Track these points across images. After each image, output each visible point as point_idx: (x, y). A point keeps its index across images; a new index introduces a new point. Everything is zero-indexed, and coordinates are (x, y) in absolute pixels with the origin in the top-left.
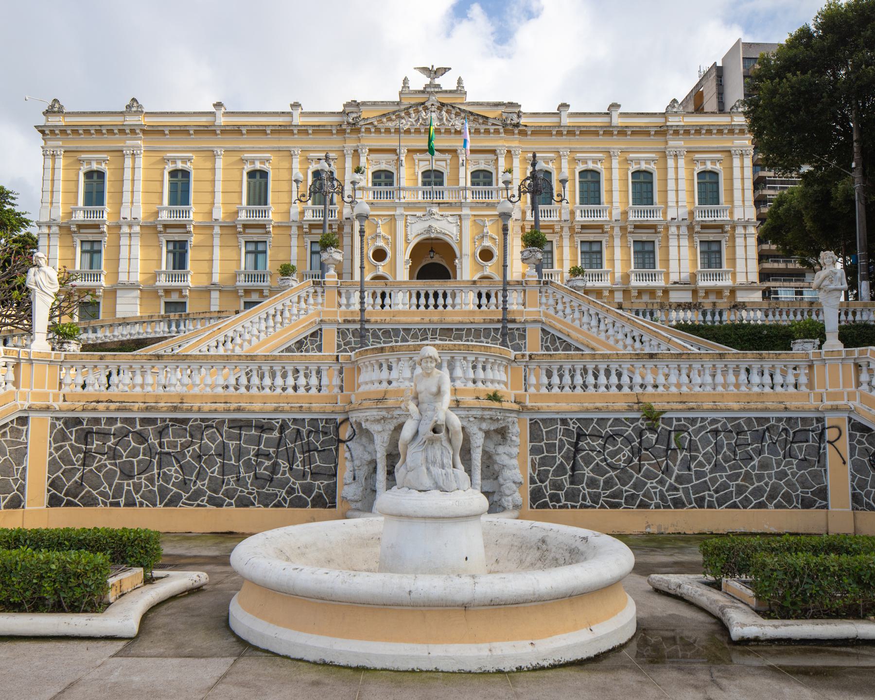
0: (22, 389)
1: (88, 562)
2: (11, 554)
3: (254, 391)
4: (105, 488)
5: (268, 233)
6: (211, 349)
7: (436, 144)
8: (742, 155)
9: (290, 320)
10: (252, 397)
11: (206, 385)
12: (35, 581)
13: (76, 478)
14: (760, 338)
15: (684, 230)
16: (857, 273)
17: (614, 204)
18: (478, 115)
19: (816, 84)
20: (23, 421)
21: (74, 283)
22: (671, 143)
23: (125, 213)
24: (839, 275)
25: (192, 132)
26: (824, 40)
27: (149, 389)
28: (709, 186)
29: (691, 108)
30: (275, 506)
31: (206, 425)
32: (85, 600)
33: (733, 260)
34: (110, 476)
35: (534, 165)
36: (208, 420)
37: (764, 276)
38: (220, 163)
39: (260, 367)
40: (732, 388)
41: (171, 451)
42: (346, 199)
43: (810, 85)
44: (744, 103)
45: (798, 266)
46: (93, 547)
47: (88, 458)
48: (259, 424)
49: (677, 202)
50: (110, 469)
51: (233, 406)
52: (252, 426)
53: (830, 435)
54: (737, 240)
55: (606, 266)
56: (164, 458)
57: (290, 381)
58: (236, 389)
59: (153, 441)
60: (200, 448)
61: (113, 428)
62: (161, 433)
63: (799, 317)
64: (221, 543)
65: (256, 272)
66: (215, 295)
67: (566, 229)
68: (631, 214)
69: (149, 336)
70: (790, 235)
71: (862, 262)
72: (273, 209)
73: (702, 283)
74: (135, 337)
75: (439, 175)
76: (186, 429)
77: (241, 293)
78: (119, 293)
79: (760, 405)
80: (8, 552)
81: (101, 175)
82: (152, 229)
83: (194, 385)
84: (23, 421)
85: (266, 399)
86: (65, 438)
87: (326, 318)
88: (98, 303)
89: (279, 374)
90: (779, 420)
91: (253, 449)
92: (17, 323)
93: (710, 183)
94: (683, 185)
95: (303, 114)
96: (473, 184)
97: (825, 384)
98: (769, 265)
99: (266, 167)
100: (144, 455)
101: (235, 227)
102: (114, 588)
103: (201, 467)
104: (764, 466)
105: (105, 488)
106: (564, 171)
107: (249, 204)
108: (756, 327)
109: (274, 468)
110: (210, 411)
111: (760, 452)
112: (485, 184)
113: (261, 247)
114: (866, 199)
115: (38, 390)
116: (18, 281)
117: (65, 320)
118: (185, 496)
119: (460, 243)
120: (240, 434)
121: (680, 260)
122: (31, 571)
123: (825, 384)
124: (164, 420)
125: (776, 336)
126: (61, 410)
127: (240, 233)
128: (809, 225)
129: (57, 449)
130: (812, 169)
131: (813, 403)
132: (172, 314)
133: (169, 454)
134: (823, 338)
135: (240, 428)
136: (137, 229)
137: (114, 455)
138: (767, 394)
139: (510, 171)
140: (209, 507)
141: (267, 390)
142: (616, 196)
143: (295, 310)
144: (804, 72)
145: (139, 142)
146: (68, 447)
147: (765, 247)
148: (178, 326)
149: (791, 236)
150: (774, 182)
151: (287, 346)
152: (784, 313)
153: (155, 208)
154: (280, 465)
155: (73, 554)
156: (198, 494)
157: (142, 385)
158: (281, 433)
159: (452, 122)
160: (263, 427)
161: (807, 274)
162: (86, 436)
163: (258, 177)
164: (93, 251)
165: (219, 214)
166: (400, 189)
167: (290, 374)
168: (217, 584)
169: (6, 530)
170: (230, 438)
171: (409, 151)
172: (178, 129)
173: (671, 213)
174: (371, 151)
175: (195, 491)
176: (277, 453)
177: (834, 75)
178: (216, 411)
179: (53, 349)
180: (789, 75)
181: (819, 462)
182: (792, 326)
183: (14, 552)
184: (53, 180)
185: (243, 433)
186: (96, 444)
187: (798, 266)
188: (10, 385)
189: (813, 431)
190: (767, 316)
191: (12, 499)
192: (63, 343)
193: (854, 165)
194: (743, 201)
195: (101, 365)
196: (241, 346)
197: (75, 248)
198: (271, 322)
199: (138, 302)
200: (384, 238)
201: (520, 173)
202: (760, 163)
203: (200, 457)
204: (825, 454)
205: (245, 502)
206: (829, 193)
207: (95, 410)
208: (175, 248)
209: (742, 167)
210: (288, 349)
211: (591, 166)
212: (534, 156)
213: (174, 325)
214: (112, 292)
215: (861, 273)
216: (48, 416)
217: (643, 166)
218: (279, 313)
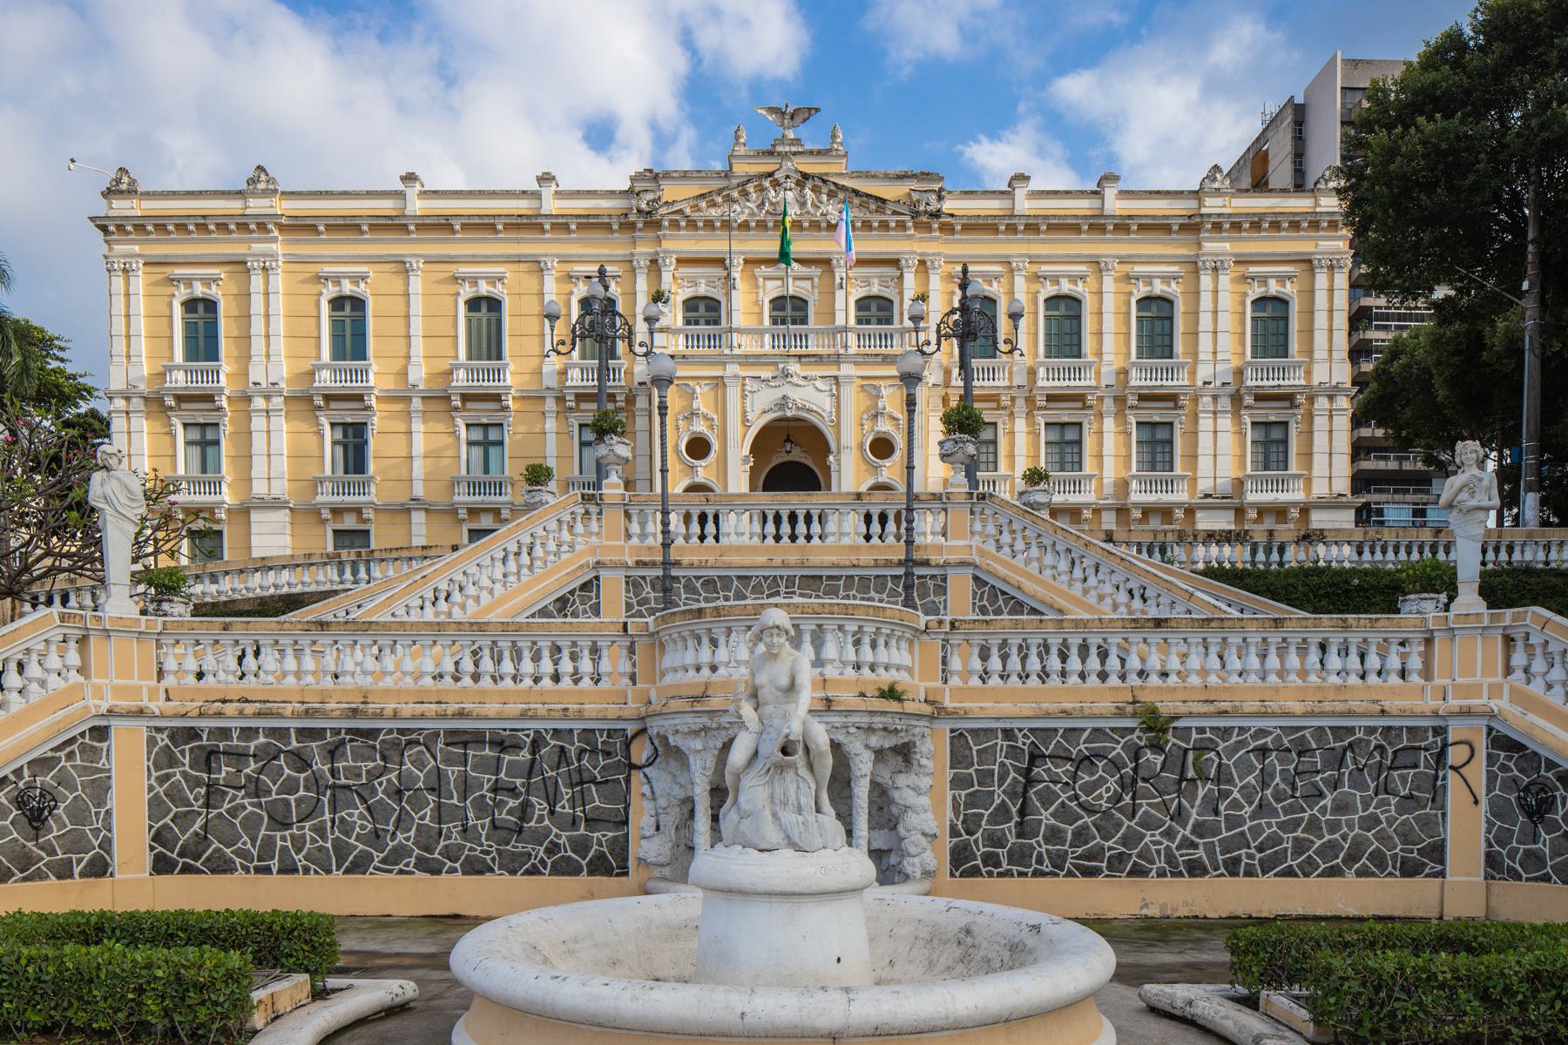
0: (94, 680)
1: (216, 966)
2: (88, 953)
3: (486, 682)
4: (245, 843)
5: (505, 409)
6: (412, 612)
7: (799, 247)
8: (1331, 268)
9: (545, 563)
10: (484, 692)
11: (405, 673)
12: (131, 996)
13: (196, 827)
14: (1347, 591)
15: (1225, 403)
16: (1518, 478)
17: (1105, 357)
18: (868, 196)
19: (1466, 136)
20: (101, 733)
21: (172, 498)
22: (1208, 246)
23: (257, 374)
24: (1486, 483)
25: (365, 228)
26: (1486, 54)
27: (309, 679)
28: (1272, 325)
29: (1246, 181)
30: (527, 873)
31: (406, 740)
32: (215, 1026)
33: (1307, 456)
34: (251, 824)
35: (963, 286)
36: (412, 731)
37: (1361, 482)
38: (417, 284)
39: (494, 642)
40: (1293, 677)
41: (351, 782)
42: (638, 349)
43: (1458, 138)
44: (1338, 173)
45: (1420, 466)
46: (225, 940)
47: (213, 794)
48: (498, 739)
49: (1215, 353)
50: (252, 813)
51: (452, 708)
52: (484, 742)
53: (1455, 755)
54: (1317, 420)
55: (1089, 467)
56: (340, 795)
57: (547, 666)
58: (457, 679)
59: (321, 766)
60: (399, 777)
61: (252, 745)
62: (333, 753)
63: (1415, 556)
64: (440, 932)
65: (486, 478)
66: (418, 518)
67: (1020, 403)
68: (1134, 373)
69: (307, 589)
70: (1408, 412)
71: (1529, 460)
72: (512, 367)
73: (1255, 496)
74: (285, 590)
75: (800, 304)
76: (374, 747)
77: (463, 514)
78: (255, 516)
79: (1339, 707)
80: (84, 950)
81: (211, 305)
82: (305, 402)
83: (384, 673)
84: (101, 733)
85: (506, 696)
86: (173, 762)
87: (602, 559)
88: (220, 533)
89: (527, 655)
90: (1371, 730)
91: (487, 779)
92: (81, 568)
93: (1273, 318)
94: (1227, 321)
95: (560, 194)
96: (859, 322)
97: (1460, 672)
98: (1366, 465)
99: (498, 291)
100: (307, 789)
101: (448, 398)
102: (262, 1007)
103: (402, 808)
104: (1342, 807)
105: (245, 843)
106: (1020, 294)
107: (470, 358)
108: (1342, 572)
109: (524, 811)
110: (414, 718)
111: (1335, 785)
112: (879, 322)
113: (493, 435)
114: (1543, 346)
115: (121, 681)
116: (76, 494)
117: (164, 562)
118: (378, 857)
119: (837, 426)
120: (465, 755)
121: (1218, 453)
122: (124, 979)
123: (1460, 672)
124: (336, 731)
125: (1373, 587)
126: (162, 716)
127: (456, 409)
128: (1442, 393)
129: (162, 780)
130: (1453, 293)
131: (1431, 703)
132: (344, 553)
133: (347, 787)
134: (1452, 589)
135: (465, 745)
136: (278, 402)
137: (257, 790)
138: (1352, 688)
139: (923, 298)
140: (419, 875)
141: (508, 682)
142: (1109, 343)
143: (559, 544)
144: (1448, 115)
145: (274, 246)
146: (178, 776)
147: (1365, 432)
148: (355, 572)
149: (1409, 413)
150: (1387, 317)
151: (540, 606)
152: (1390, 549)
153: (307, 365)
154: (533, 806)
155: (192, 952)
156: (398, 854)
157: (293, 675)
158: (533, 753)
159: (823, 209)
160: (503, 744)
161: (1434, 481)
162: (207, 759)
163: (486, 307)
164: (205, 442)
165: (419, 374)
166: (731, 330)
167: (546, 654)
168: (432, 999)
169: (82, 914)
170: (449, 761)
171: (746, 261)
172: (341, 222)
173: (1204, 372)
174: (679, 261)
175: (394, 849)
176: (528, 786)
177: (1503, 120)
178: (422, 717)
179: (144, 612)
180: (1421, 120)
181: (1433, 800)
182: (1398, 571)
183: (94, 950)
184: (128, 316)
185: (471, 753)
186: (224, 772)
187: (1420, 466)
188: (73, 672)
189: (1426, 749)
190: (1360, 553)
191: (92, 863)
192: (161, 601)
193: (1525, 285)
194: (1330, 351)
195: (226, 640)
196: (463, 607)
197: (174, 437)
198: (512, 566)
199: (288, 531)
200: (706, 417)
201: (941, 300)
202: (1362, 281)
203: (399, 792)
204: (1444, 787)
205: (478, 866)
206: (1480, 337)
207: (219, 714)
208: (345, 436)
209: (1331, 290)
210: (544, 613)
211: (1066, 287)
212: (965, 271)
213: (348, 570)
214: (243, 511)
215: (1527, 477)
216: (141, 726)
217: (1159, 288)
218: (525, 550)
